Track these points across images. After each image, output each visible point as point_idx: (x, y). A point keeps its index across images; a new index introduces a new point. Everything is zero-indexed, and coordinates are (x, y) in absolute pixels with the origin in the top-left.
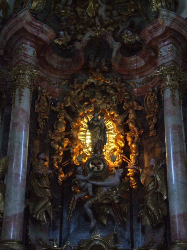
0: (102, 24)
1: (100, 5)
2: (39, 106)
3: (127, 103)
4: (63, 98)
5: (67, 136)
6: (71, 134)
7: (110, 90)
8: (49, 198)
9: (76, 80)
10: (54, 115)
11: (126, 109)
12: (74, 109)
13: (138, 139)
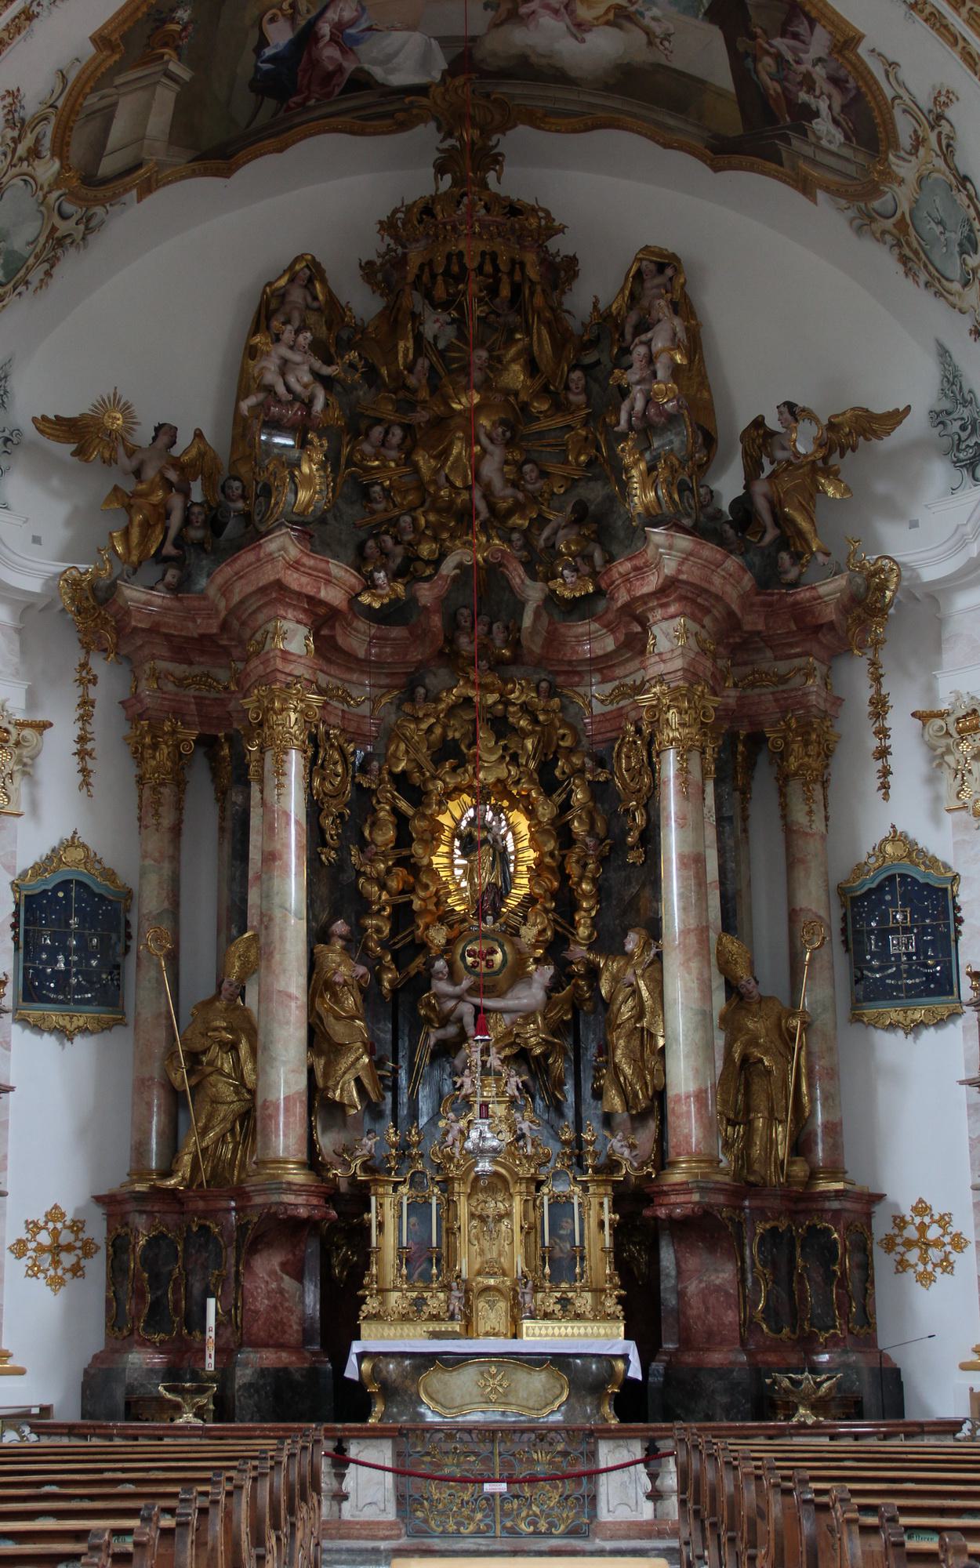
1: (484, 451)
2: (323, 779)
3: (568, 760)
4: (387, 749)
5: (399, 862)
6: (412, 856)
7: (520, 718)
8: (364, 1044)
9: (421, 691)
11: (565, 777)
13: (597, 869)
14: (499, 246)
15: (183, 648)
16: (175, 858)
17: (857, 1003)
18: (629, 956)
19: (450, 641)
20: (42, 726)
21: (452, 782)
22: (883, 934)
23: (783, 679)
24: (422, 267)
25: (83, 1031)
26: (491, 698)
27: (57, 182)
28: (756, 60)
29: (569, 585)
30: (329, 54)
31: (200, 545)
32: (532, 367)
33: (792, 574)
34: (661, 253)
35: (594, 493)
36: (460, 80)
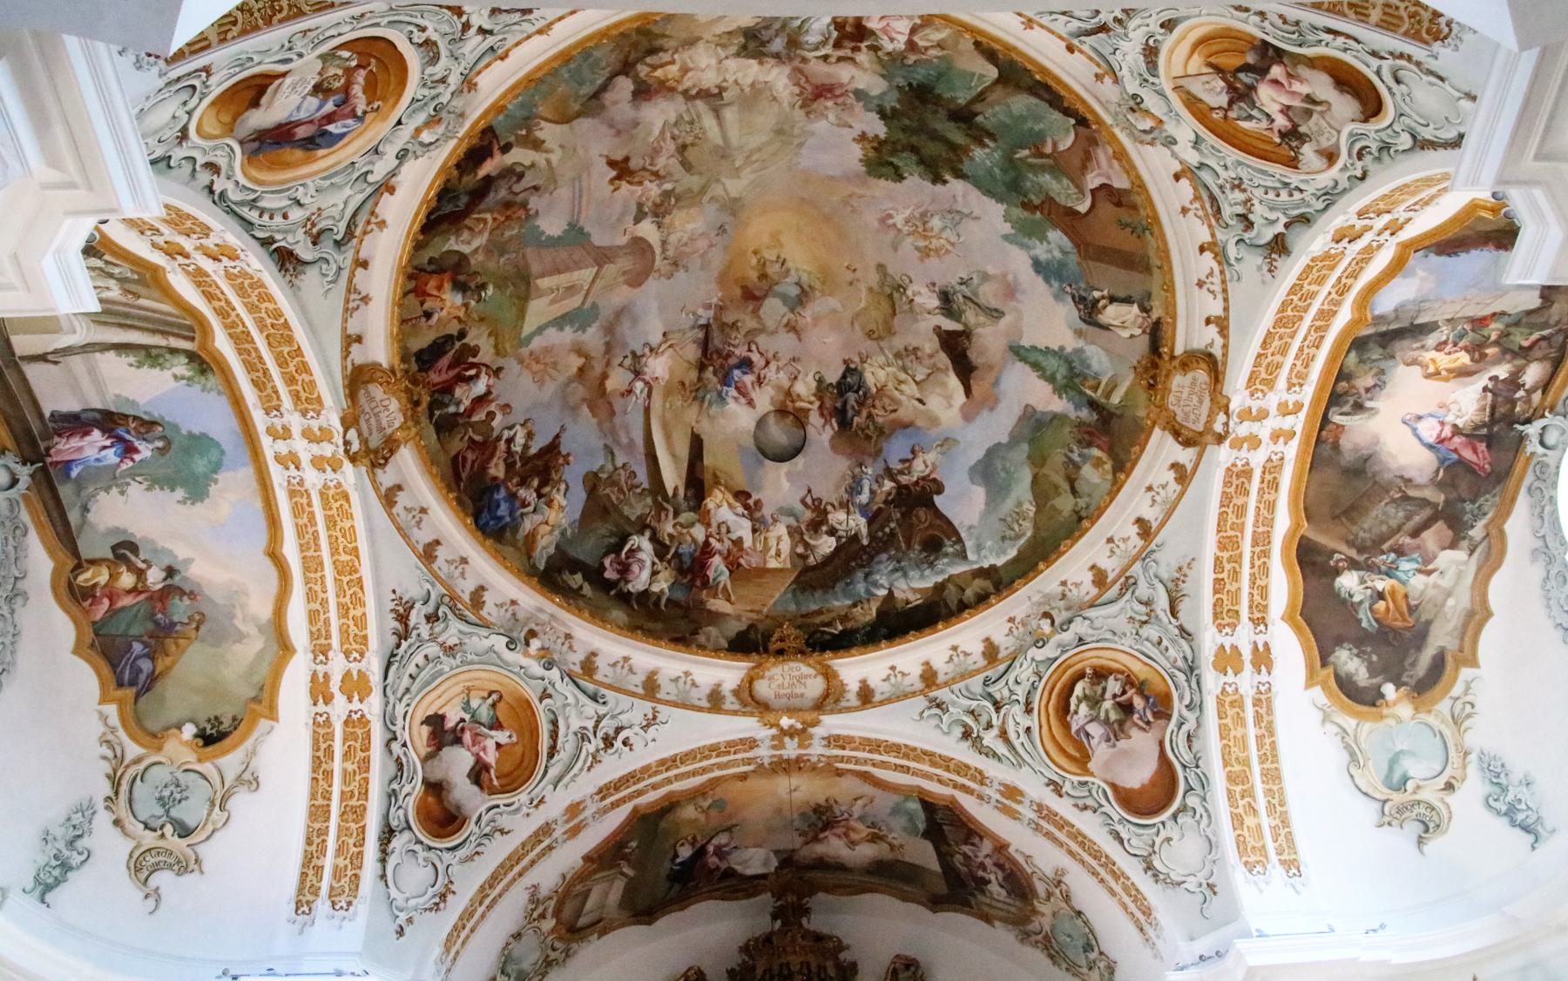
14: (811, 959)
24: (765, 972)
27: (553, 931)
28: (952, 856)
30: (713, 860)
34: (906, 958)
36: (785, 871)
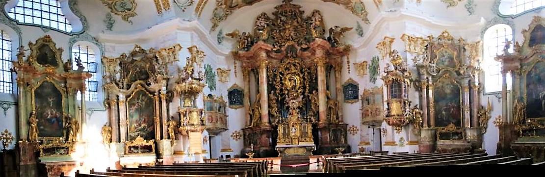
0: (292, 39)
5: (281, 83)
10: (275, 76)
12: (282, 72)
15: (248, 58)
16: (249, 85)
17: (345, 100)
18: (313, 94)
19: (287, 55)
20: (230, 70)
21: (288, 72)
22: (348, 91)
23: (335, 59)
25: (238, 108)
26: (293, 62)
29: (304, 46)
31: (250, 46)
32: (298, 22)
33: (336, 46)
35: (307, 37)
